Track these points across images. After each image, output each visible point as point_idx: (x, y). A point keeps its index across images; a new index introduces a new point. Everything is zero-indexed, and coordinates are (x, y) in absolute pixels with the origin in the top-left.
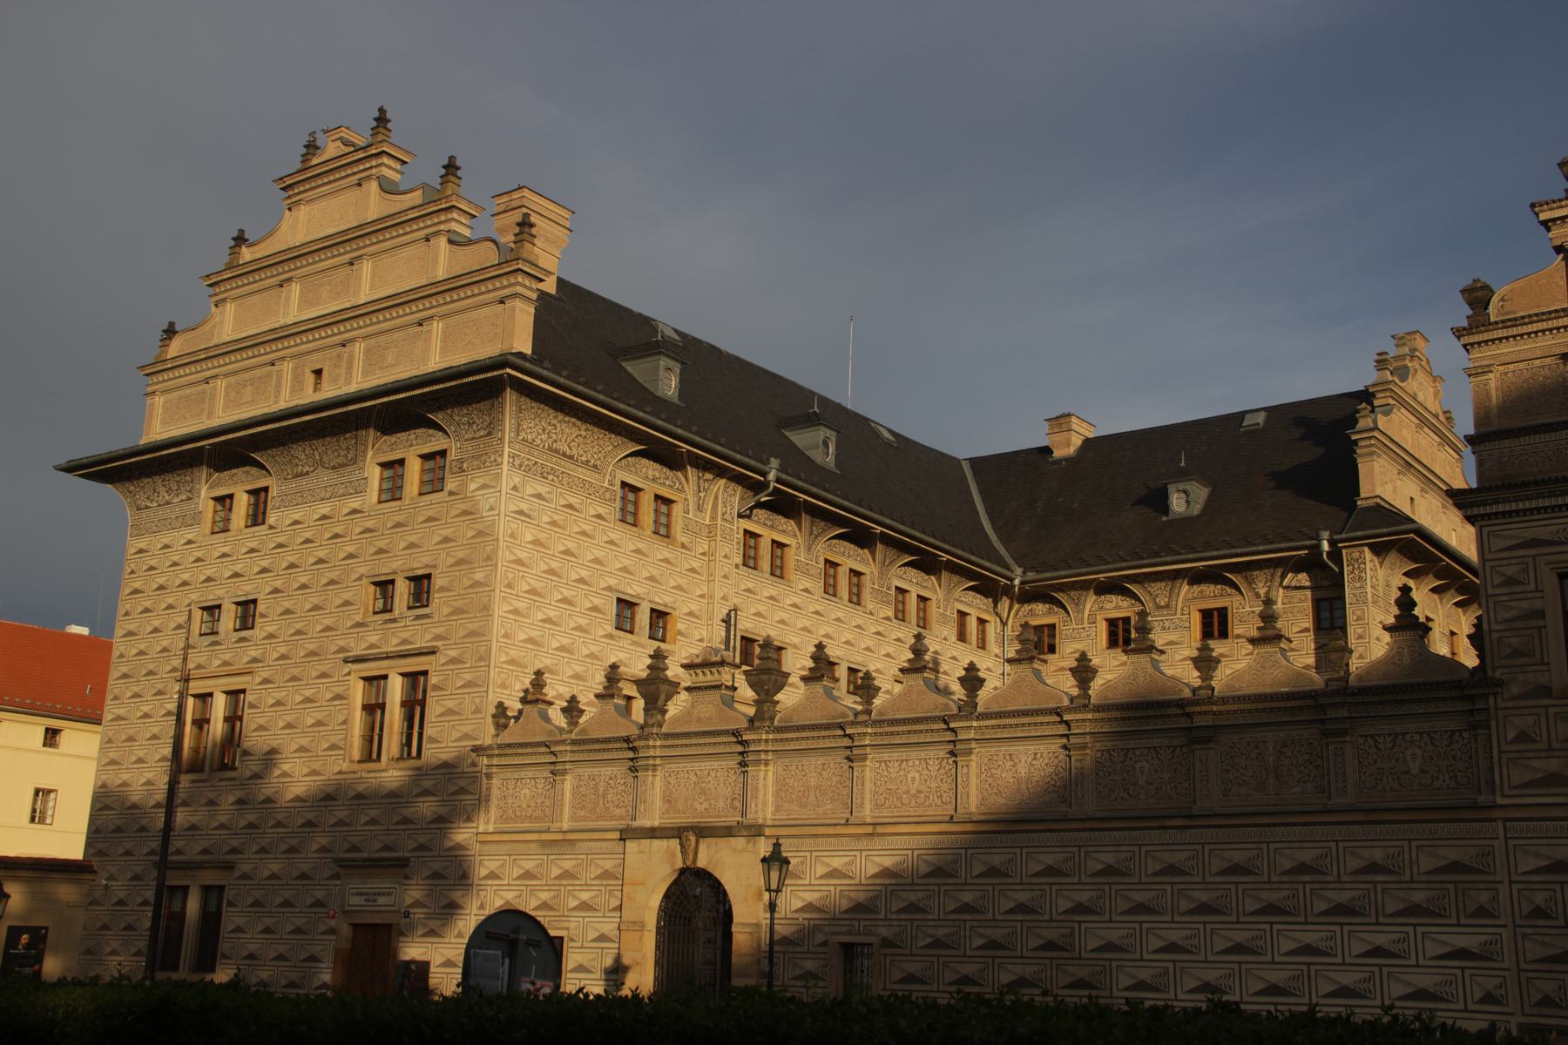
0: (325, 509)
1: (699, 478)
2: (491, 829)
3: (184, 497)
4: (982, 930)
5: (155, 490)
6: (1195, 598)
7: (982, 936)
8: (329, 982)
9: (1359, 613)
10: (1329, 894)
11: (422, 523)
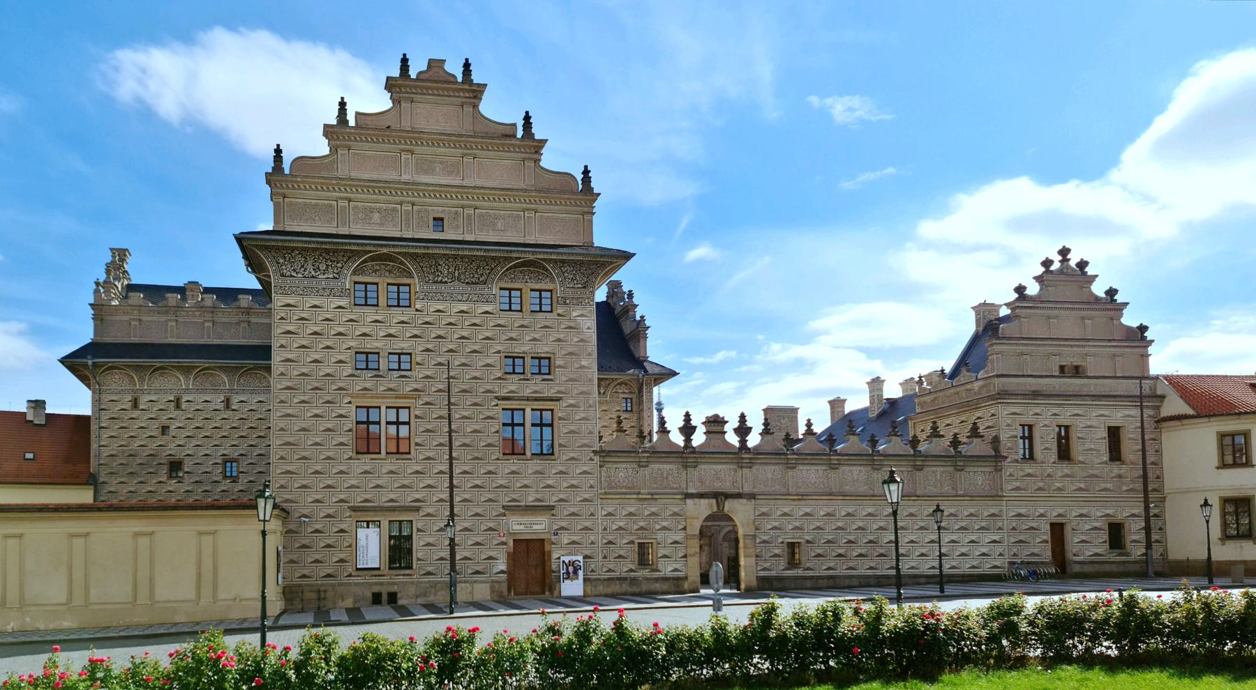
0: (464, 308)
2: (603, 491)
3: (331, 276)
4: (846, 537)
5: (302, 267)
7: (846, 539)
8: (505, 570)
10: (960, 523)
11: (541, 328)
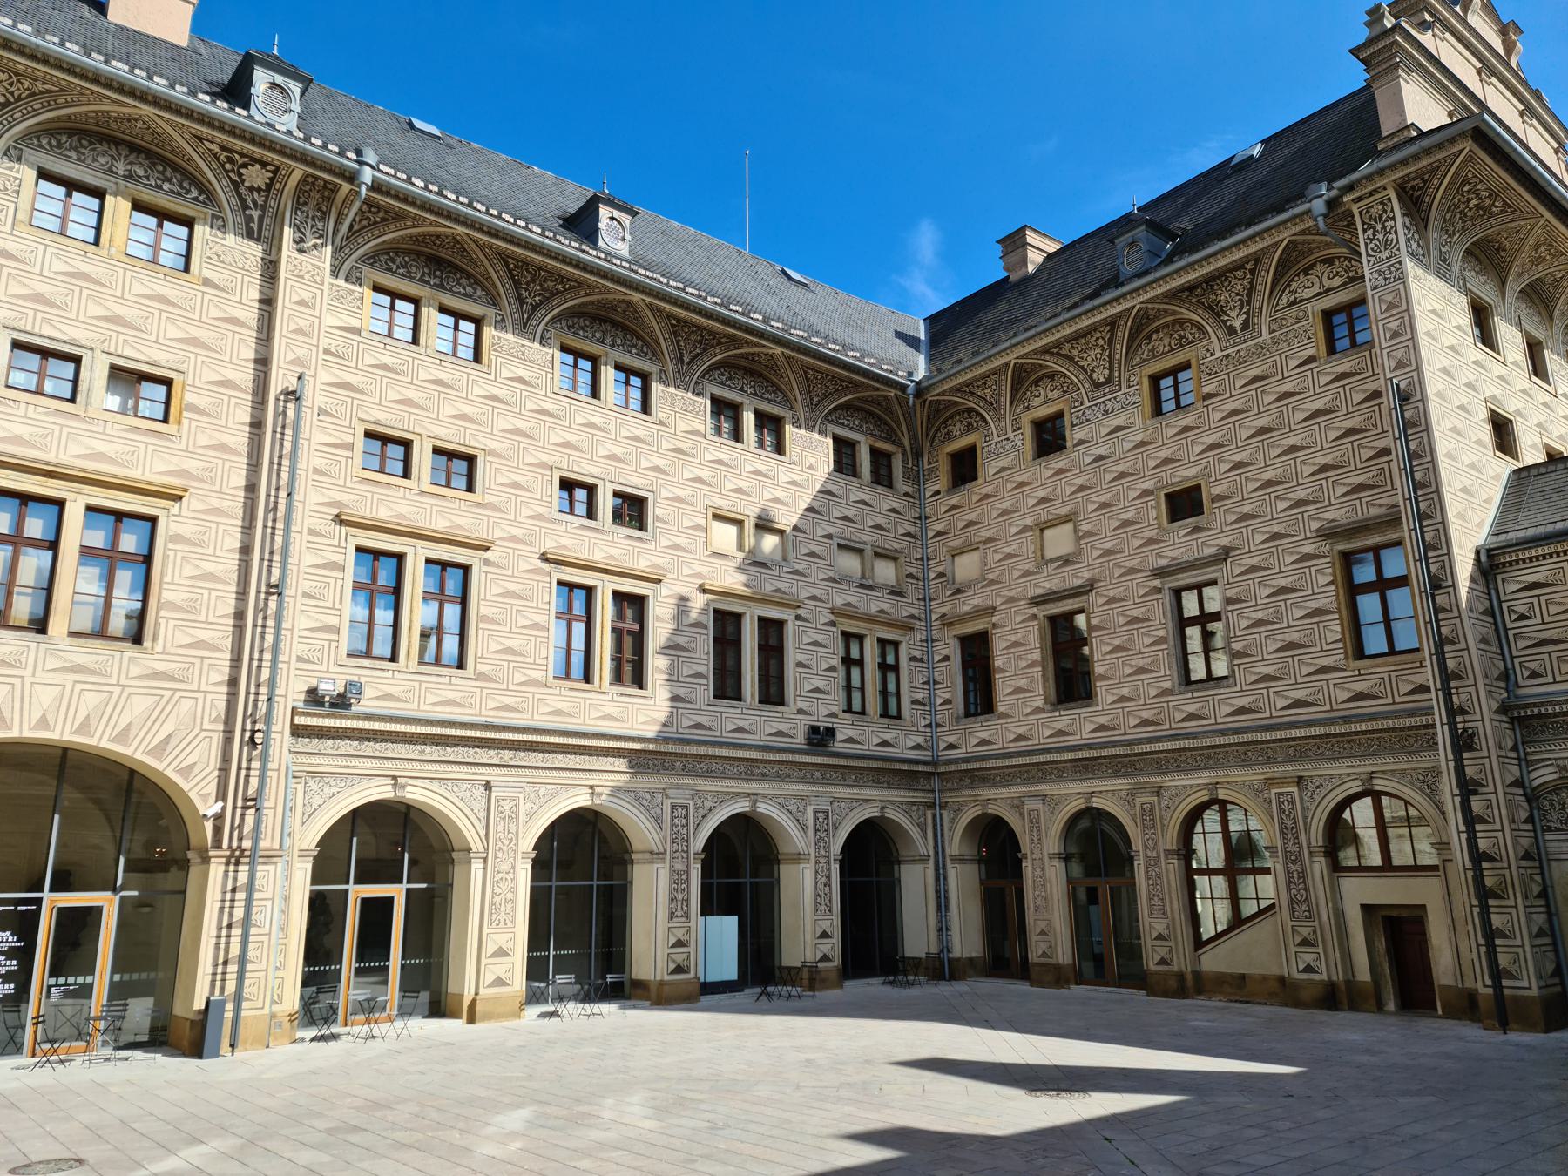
1: (236, 185)
6: (1145, 360)
9: (1389, 298)
